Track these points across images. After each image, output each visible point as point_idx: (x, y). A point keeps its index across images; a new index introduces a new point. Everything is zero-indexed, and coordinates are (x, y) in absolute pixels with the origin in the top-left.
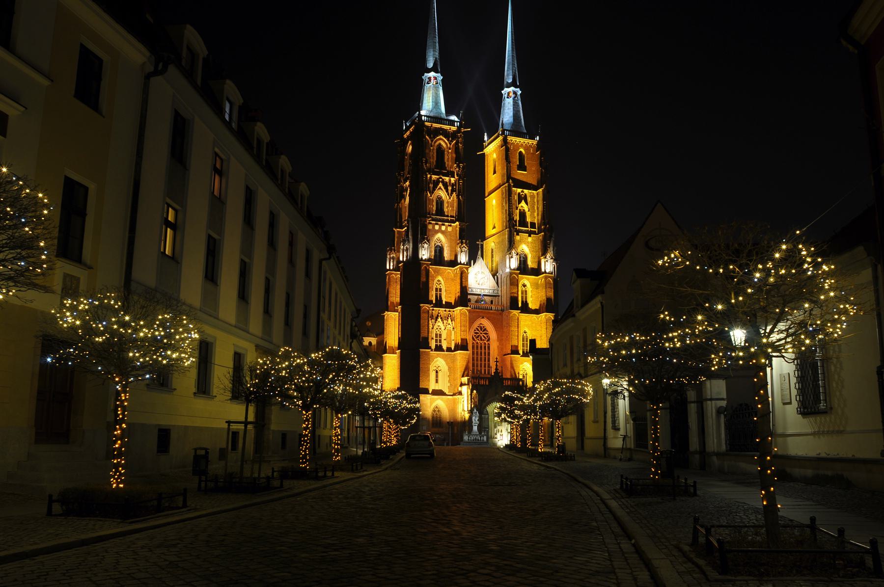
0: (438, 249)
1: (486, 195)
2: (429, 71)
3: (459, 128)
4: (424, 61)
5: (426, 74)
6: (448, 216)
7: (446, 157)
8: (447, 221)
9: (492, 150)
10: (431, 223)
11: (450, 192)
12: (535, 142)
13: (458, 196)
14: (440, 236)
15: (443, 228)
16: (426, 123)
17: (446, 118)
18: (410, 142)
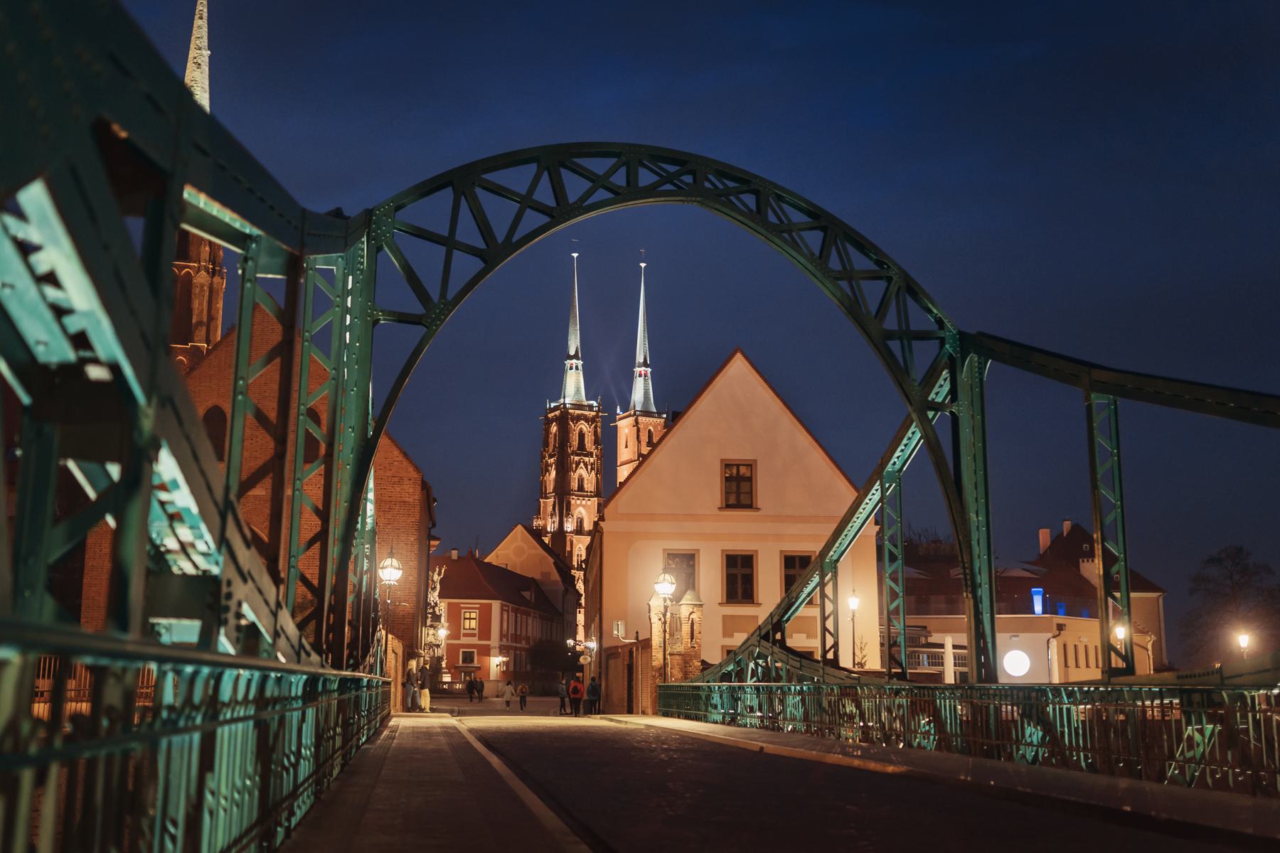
0: (579, 520)
1: (618, 464)
2: (571, 358)
3: (598, 412)
4: (566, 346)
5: (568, 361)
6: (587, 492)
7: (586, 440)
8: (587, 496)
9: (625, 427)
10: (573, 499)
11: (589, 470)
12: (663, 421)
13: (596, 474)
14: (581, 509)
15: (584, 502)
16: (570, 411)
17: (586, 403)
18: (554, 423)
